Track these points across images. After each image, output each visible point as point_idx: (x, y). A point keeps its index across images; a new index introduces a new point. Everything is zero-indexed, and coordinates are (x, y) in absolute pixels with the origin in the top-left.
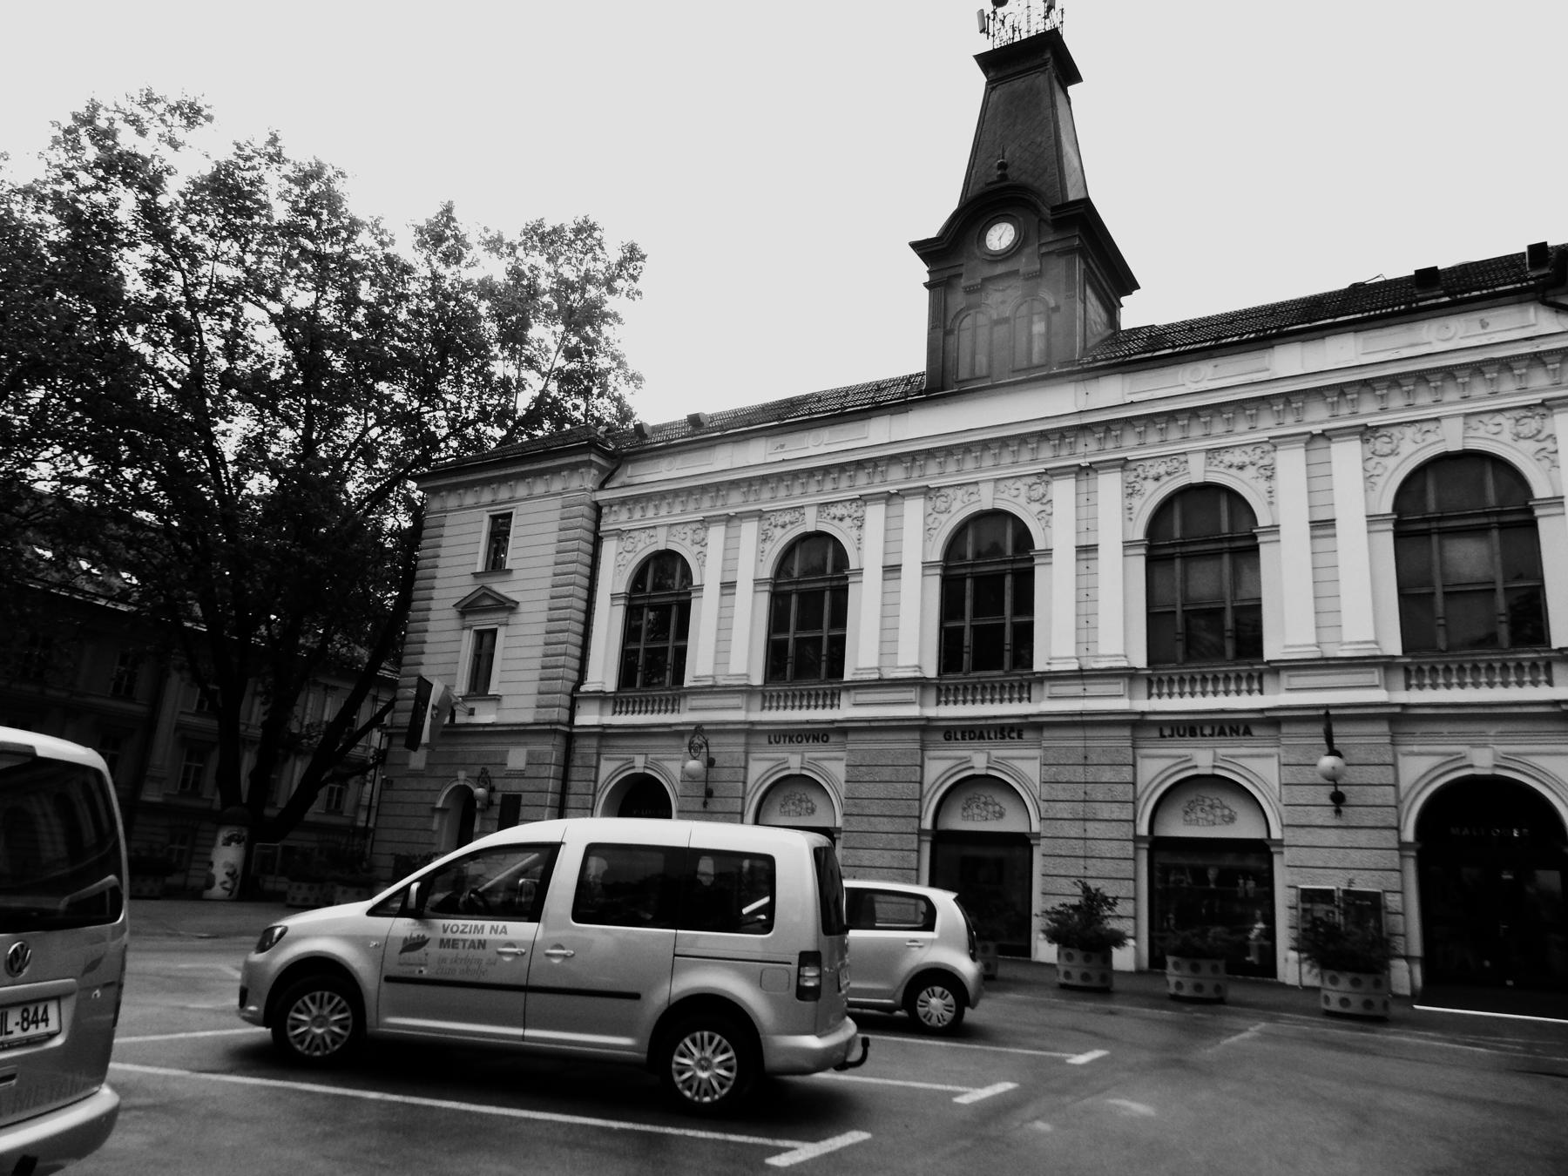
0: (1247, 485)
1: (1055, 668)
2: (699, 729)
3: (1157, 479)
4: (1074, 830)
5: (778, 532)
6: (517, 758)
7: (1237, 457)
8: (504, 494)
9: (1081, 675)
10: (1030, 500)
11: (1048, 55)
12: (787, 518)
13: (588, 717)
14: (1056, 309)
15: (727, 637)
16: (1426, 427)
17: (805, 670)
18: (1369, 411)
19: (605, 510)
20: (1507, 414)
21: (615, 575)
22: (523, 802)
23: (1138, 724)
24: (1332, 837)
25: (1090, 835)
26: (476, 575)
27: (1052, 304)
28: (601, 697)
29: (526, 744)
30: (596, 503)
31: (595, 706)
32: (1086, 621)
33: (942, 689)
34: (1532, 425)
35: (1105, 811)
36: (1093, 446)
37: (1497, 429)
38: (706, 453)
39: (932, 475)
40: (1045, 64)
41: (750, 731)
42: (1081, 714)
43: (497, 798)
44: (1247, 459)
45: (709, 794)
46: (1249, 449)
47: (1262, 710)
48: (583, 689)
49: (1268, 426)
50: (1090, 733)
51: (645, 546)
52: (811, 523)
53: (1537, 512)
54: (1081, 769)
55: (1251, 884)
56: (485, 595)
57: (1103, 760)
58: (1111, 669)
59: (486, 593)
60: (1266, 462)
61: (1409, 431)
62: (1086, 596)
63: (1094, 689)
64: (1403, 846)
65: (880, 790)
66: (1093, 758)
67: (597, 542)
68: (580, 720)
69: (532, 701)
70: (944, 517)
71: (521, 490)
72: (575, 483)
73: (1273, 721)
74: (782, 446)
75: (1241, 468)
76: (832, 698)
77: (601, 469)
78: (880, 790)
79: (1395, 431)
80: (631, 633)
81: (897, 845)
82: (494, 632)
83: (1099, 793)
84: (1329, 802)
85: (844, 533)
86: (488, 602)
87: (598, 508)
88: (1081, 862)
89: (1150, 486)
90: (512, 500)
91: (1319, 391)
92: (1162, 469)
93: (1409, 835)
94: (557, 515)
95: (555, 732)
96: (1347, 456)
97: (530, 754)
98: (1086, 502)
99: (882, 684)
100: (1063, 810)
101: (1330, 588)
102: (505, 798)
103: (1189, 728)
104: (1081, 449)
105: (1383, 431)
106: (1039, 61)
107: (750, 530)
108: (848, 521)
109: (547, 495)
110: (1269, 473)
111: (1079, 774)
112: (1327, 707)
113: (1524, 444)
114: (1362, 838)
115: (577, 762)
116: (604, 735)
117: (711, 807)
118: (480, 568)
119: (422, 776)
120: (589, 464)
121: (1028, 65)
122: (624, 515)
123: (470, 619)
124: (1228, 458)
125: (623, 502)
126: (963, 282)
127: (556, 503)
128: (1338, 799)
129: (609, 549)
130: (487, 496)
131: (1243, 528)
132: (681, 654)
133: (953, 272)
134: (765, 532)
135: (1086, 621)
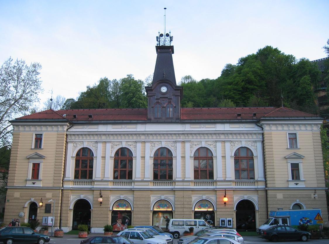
2: (100, 190)
3: (196, 145)
4: (181, 210)
5: (115, 146)
6: (49, 195)
7: (210, 143)
8: (38, 129)
12: (117, 144)
13: (66, 186)
14: (175, 107)
15: (104, 168)
20: (251, 142)
23: (193, 190)
24: (224, 210)
25: (184, 210)
27: (174, 106)
28: (69, 181)
29: (52, 192)
32: (184, 171)
35: (187, 206)
36: (184, 138)
37: (249, 144)
39: (151, 138)
40: (170, 52)
41: (111, 190)
42: (183, 188)
43: (44, 205)
44: (211, 144)
46: (212, 142)
47: (214, 189)
48: (65, 179)
50: (185, 192)
51: (80, 147)
52: (124, 145)
53: (254, 158)
54: (182, 199)
59: (37, 154)
60: (214, 145)
61: (236, 142)
62: (184, 166)
63: (184, 184)
64: (234, 211)
68: (65, 186)
69: (52, 181)
70: (153, 147)
71: (44, 128)
72: (60, 129)
75: (210, 145)
76: (131, 183)
77: (68, 126)
80: (77, 165)
82: (39, 164)
83: (185, 203)
84: (224, 204)
87: (67, 135)
88: (183, 215)
89: (194, 146)
90: (41, 131)
93: (235, 209)
98: (184, 148)
100: (179, 206)
101: (224, 168)
102: (46, 205)
104: (182, 137)
105: (233, 142)
106: (168, 51)
108: (132, 146)
109: (53, 131)
110: (215, 147)
111: (182, 199)
112: (225, 188)
114: (229, 210)
115: (65, 196)
116: (72, 190)
117: (102, 206)
119: (19, 199)
120: (66, 125)
123: (30, 160)
126: (156, 97)
129: (70, 146)
130: (33, 128)
131: (209, 155)
133: (153, 94)
135: (184, 171)
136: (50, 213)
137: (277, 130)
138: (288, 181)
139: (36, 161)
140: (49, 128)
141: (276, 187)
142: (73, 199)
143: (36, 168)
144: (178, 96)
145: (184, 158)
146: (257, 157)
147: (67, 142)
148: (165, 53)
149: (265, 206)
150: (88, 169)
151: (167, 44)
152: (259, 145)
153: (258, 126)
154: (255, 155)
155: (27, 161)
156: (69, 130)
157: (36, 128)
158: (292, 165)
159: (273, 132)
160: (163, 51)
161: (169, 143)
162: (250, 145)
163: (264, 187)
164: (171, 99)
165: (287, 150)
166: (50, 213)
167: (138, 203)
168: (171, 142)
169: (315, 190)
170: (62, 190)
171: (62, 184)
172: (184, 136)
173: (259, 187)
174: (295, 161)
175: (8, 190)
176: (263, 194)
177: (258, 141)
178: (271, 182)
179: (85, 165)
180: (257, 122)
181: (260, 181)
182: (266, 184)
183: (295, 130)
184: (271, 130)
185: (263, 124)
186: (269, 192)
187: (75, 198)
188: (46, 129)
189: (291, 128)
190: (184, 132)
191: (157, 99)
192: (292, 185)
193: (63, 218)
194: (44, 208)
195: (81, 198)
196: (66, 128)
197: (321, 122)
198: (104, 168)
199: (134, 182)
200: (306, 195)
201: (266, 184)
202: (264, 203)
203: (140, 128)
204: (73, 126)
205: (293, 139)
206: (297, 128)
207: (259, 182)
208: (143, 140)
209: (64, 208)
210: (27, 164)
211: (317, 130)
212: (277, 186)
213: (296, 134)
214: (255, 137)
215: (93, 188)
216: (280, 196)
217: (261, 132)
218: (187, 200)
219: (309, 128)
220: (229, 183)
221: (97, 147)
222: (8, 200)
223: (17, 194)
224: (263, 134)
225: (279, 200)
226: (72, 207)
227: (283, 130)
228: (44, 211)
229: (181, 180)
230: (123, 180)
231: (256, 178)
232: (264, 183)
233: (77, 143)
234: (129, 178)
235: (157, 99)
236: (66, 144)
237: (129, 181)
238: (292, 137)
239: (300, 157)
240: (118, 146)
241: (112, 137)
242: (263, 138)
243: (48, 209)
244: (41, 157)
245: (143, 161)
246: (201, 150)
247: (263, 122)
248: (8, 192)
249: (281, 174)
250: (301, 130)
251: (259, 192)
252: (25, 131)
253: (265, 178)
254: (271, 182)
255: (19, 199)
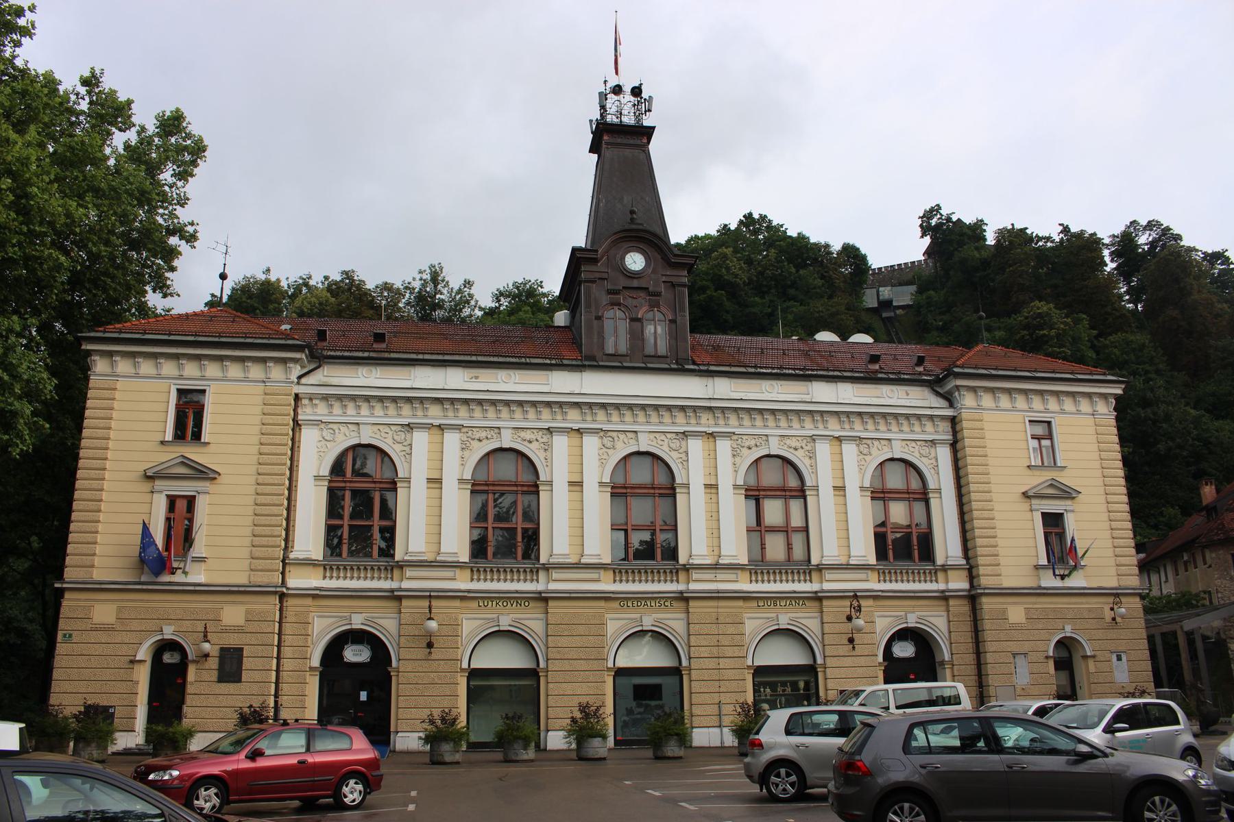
0: (799, 458)
1: (696, 562)
2: (430, 596)
4: (712, 663)
5: (475, 444)
6: (233, 614)
7: (793, 443)
8: (191, 369)
9: (716, 567)
10: (671, 449)
11: (645, 141)
12: (483, 434)
13: (298, 580)
14: (673, 321)
15: (434, 519)
16: (883, 442)
17: (506, 550)
18: (858, 429)
19: (305, 402)
21: (316, 457)
22: (245, 654)
24: (848, 661)
26: (162, 443)
28: (308, 563)
29: (242, 603)
30: (297, 395)
31: (309, 570)
33: (618, 570)
34: (925, 451)
35: (729, 652)
36: (712, 422)
38: (407, 369)
41: (464, 597)
45: (430, 645)
48: (292, 556)
49: (809, 428)
55: (768, 690)
56: (182, 463)
57: (727, 620)
58: (731, 564)
59: (186, 462)
60: (809, 448)
62: (714, 516)
63: (720, 576)
65: (577, 641)
66: (721, 619)
67: (297, 424)
68: (293, 582)
70: (610, 452)
71: (212, 370)
72: (276, 372)
73: (818, 598)
74: (477, 378)
75: (796, 449)
78: (577, 641)
79: (869, 442)
80: (333, 509)
81: (591, 679)
82: (191, 501)
83: (725, 641)
85: (534, 452)
86: (183, 470)
88: (717, 683)
89: (745, 451)
90: (203, 378)
91: (837, 414)
92: (752, 443)
94: (259, 400)
95: (276, 592)
96: (849, 450)
97: (247, 612)
98: (713, 456)
99: (578, 566)
100: (704, 652)
103: (773, 599)
104: (704, 421)
106: (638, 142)
107: (452, 440)
108: (534, 445)
109: (246, 380)
110: (812, 455)
111: (714, 629)
112: (854, 591)
113: (924, 460)
114: (862, 661)
116: (316, 595)
117: (434, 656)
118: (169, 436)
119: (113, 630)
120: (295, 361)
121: (632, 142)
122: (322, 409)
124: (788, 442)
125: (325, 398)
127: (261, 387)
128: (851, 640)
129: (309, 437)
130: (169, 368)
132: (389, 533)
133: (598, 275)
134: (463, 442)
136: (239, 680)
137: (998, 409)
138: (1037, 567)
139: (184, 488)
140: (234, 370)
141: (1005, 585)
142: (322, 627)
143: (182, 512)
144: (684, 285)
145: (713, 491)
146: (939, 491)
147: (297, 424)
148: (621, 145)
149: (970, 647)
150: (377, 522)
151: (629, 119)
152: (944, 454)
153: (938, 394)
154: (932, 485)
155: (147, 486)
156: (303, 381)
157: (180, 367)
158: (1045, 516)
159: (986, 416)
160: (619, 140)
161: (663, 437)
162: (917, 455)
163: (966, 585)
164: (658, 294)
165: (1028, 472)
166: (239, 680)
167: (563, 642)
168: (669, 436)
169: (1116, 595)
170: (282, 596)
171: (283, 573)
172: (711, 416)
173: (953, 585)
174: (1053, 507)
175: (67, 595)
176: (960, 608)
177: (942, 442)
178: (989, 570)
179: (362, 508)
180: (935, 384)
181: (955, 568)
182: (972, 577)
183: (1047, 411)
184: (979, 407)
185: (957, 387)
186: (987, 603)
187: (330, 626)
188: (219, 374)
189: (1037, 403)
190: (714, 404)
191: (610, 292)
192: (1049, 581)
193: (283, 700)
194: (213, 663)
195: (354, 627)
196: (296, 370)
197: (1120, 392)
198: (434, 519)
199: (547, 568)
200: (1090, 610)
201: (972, 577)
202: (968, 638)
203: (563, 383)
204: (319, 367)
205: (1045, 431)
206: (1053, 404)
207: (949, 572)
208: (576, 426)
209: (287, 664)
210: (147, 497)
211: (1106, 411)
212: (1007, 582)
213: (1049, 423)
214: (929, 427)
215: (400, 590)
216: (1016, 613)
217: (950, 412)
218: (731, 629)
219: (1085, 406)
220: (861, 575)
221: (411, 445)
222: (65, 635)
223: (104, 611)
224: (954, 421)
225: (1016, 627)
226: (316, 662)
227: (1014, 409)
228: (216, 673)
229: (708, 562)
230: (508, 563)
231: (940, 560)
232: (965, 573)
233: (335, 427)
234: (526, 556)
235: (610, 292)
236: (293, 430)
237: (528, 565)
238: (1039, 430)
239: (1067, 494)
240: (485, 441)
241: (463, 411)
242: (955, 433)
243: (231, 665)
244: (203, 473)
245: (576, 495)
246: (764, 464)
247: (959, 382)
248: (65, 603)
249: (1015, 550)
250: (1063, 412)
251: (951, 602)
252: (137, 376)
253: (966, 557)
254: (989, 570)
255: (113, 630)
